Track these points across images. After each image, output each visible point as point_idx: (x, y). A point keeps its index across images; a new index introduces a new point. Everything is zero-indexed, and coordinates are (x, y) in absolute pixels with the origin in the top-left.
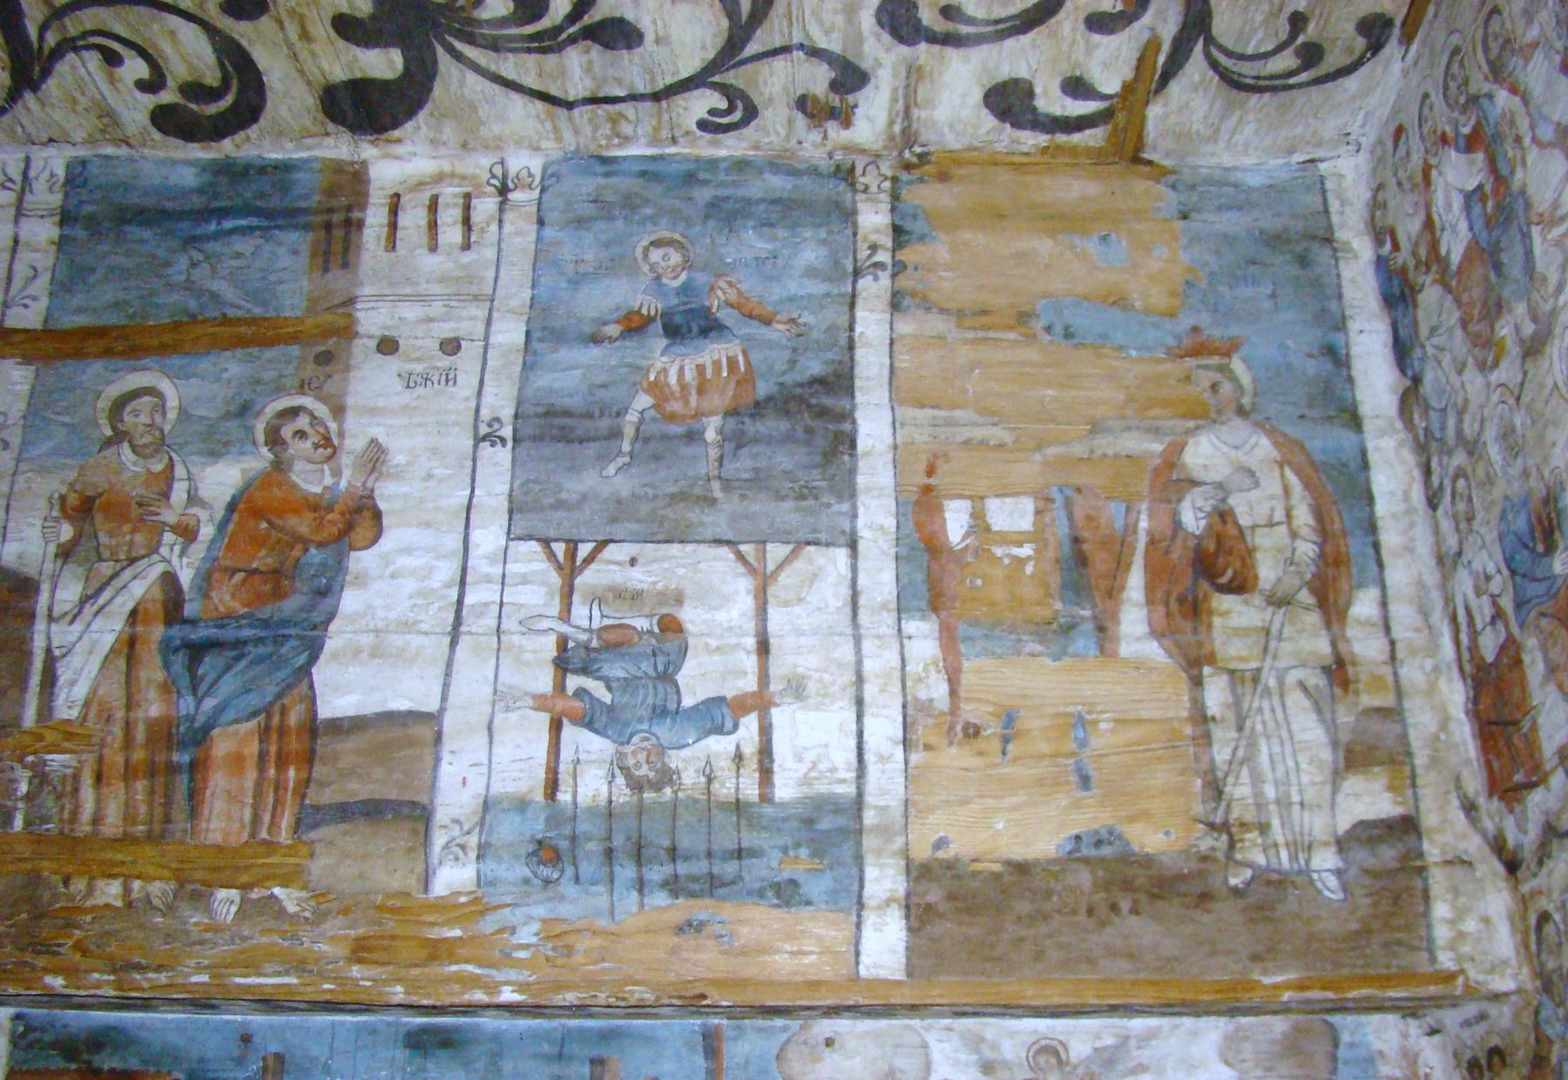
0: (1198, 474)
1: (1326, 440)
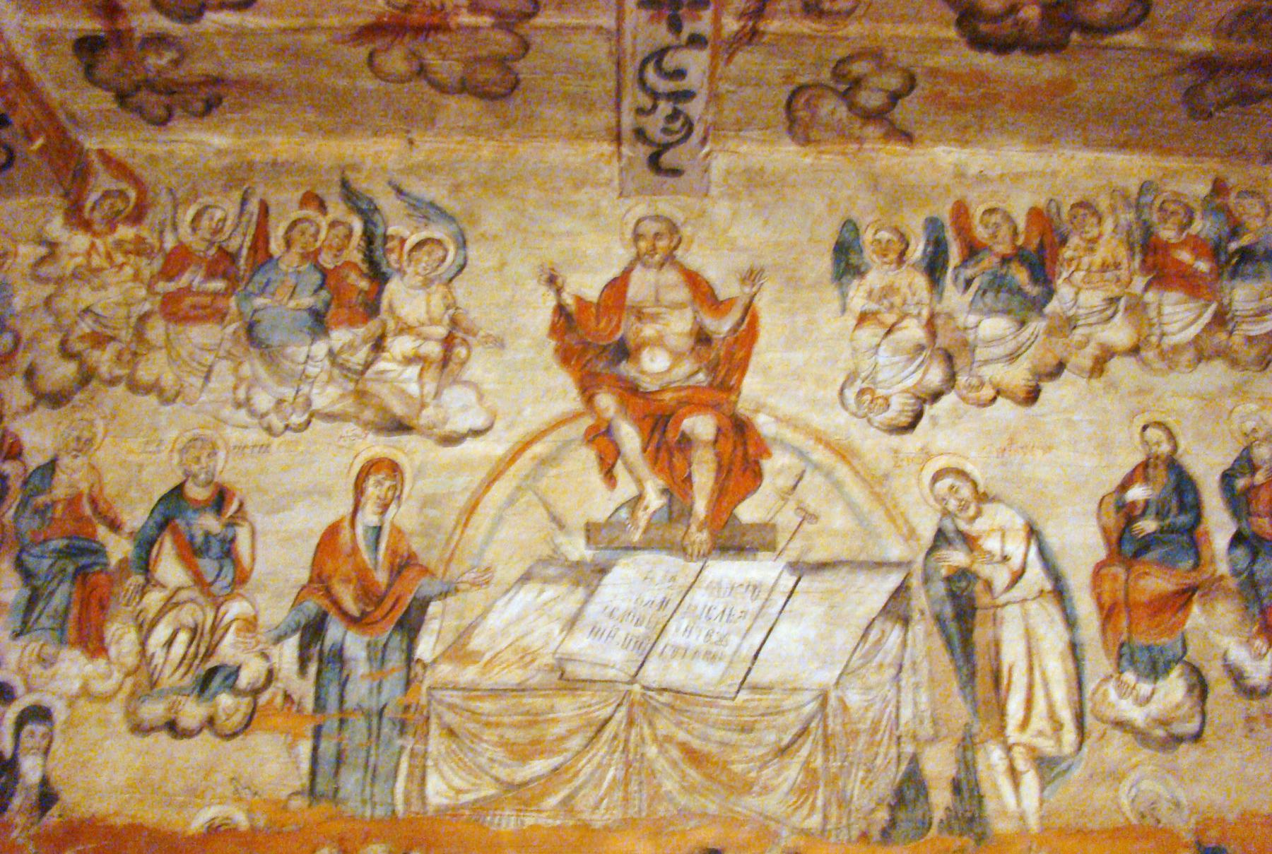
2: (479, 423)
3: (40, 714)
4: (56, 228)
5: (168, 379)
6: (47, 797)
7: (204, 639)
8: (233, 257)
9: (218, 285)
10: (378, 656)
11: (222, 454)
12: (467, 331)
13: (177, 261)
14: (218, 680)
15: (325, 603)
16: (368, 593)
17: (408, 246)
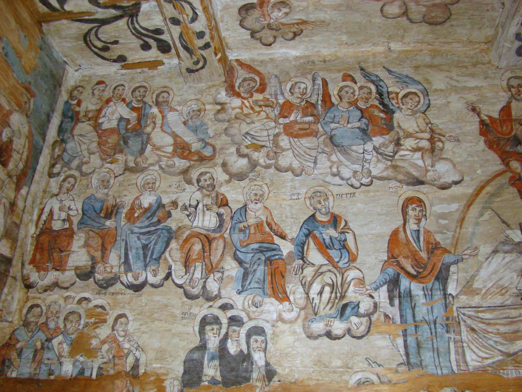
0: (11, 126)
1: (38, 138)
2: (456, 178)
3: (259, 331)
4: (223, 96)
5: (296, 164)
6: (270, 374)
7: (338, 290)
8: (314, 106)
9: (310, 119)
10: (429, 294)
11: (331, 199)
12: (440, 134)
13: (286, 109)
14: (348, 310)
15: (399, 270)
16: (417, 262)
17: (400, 96)
